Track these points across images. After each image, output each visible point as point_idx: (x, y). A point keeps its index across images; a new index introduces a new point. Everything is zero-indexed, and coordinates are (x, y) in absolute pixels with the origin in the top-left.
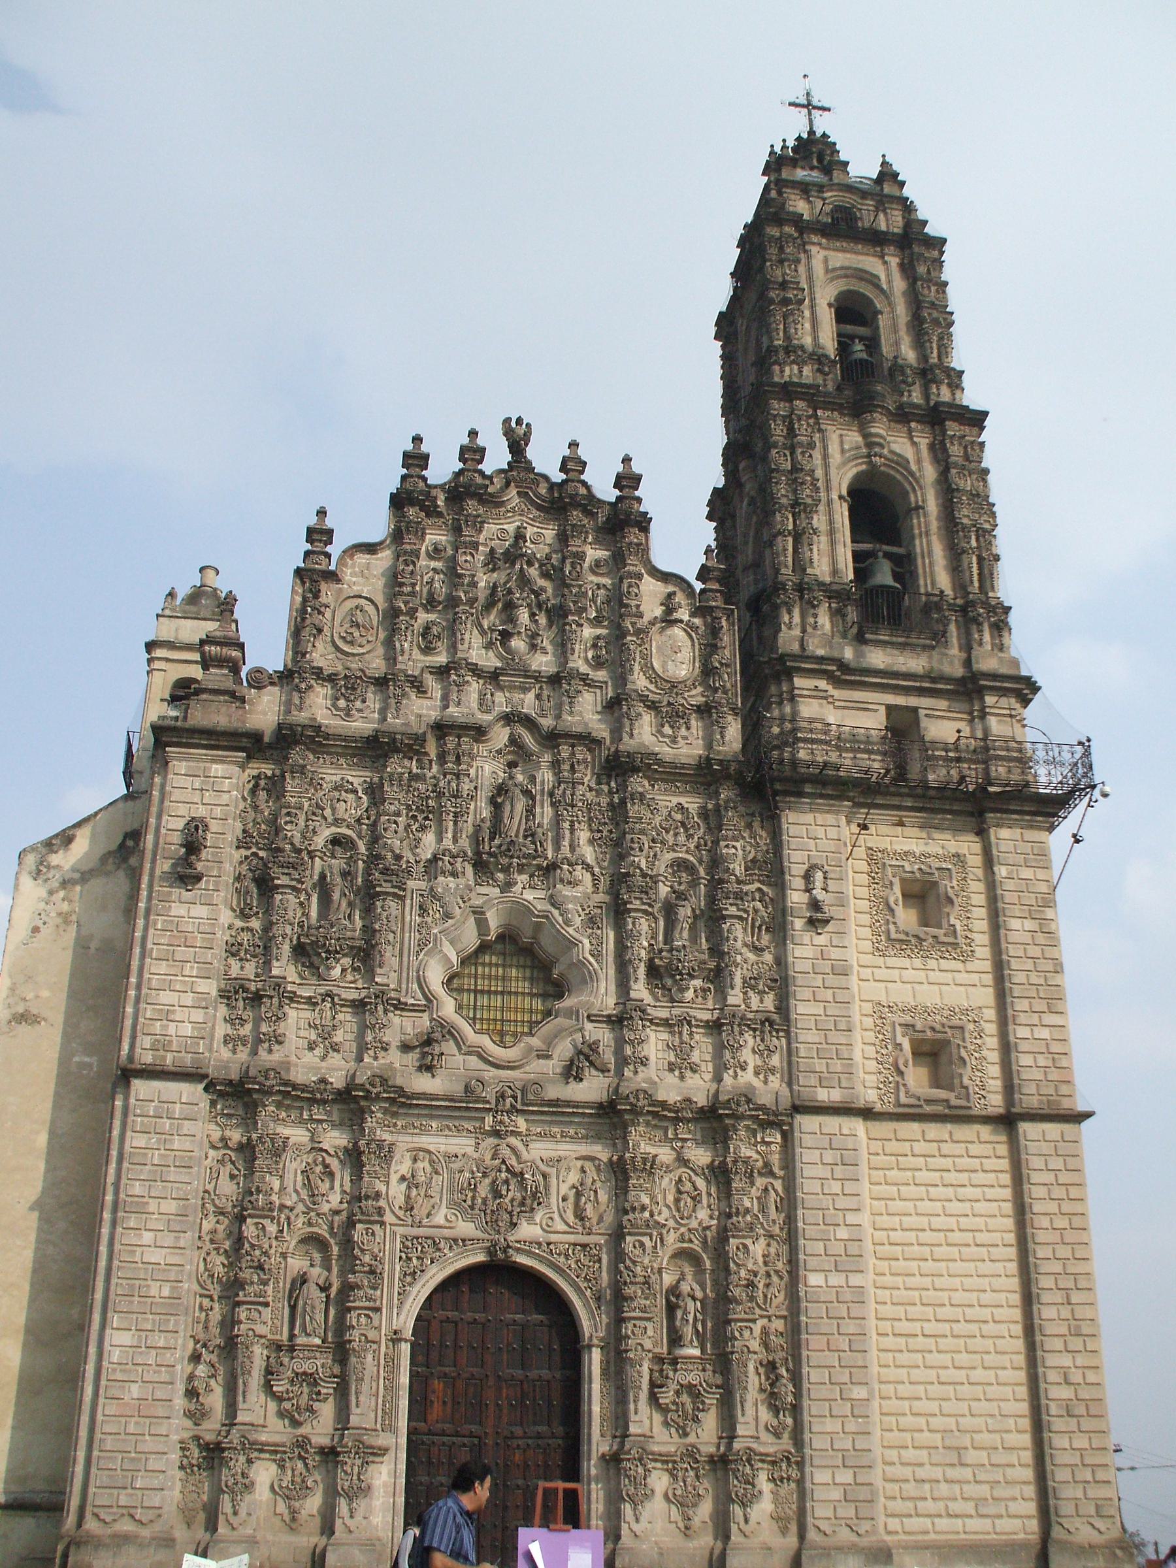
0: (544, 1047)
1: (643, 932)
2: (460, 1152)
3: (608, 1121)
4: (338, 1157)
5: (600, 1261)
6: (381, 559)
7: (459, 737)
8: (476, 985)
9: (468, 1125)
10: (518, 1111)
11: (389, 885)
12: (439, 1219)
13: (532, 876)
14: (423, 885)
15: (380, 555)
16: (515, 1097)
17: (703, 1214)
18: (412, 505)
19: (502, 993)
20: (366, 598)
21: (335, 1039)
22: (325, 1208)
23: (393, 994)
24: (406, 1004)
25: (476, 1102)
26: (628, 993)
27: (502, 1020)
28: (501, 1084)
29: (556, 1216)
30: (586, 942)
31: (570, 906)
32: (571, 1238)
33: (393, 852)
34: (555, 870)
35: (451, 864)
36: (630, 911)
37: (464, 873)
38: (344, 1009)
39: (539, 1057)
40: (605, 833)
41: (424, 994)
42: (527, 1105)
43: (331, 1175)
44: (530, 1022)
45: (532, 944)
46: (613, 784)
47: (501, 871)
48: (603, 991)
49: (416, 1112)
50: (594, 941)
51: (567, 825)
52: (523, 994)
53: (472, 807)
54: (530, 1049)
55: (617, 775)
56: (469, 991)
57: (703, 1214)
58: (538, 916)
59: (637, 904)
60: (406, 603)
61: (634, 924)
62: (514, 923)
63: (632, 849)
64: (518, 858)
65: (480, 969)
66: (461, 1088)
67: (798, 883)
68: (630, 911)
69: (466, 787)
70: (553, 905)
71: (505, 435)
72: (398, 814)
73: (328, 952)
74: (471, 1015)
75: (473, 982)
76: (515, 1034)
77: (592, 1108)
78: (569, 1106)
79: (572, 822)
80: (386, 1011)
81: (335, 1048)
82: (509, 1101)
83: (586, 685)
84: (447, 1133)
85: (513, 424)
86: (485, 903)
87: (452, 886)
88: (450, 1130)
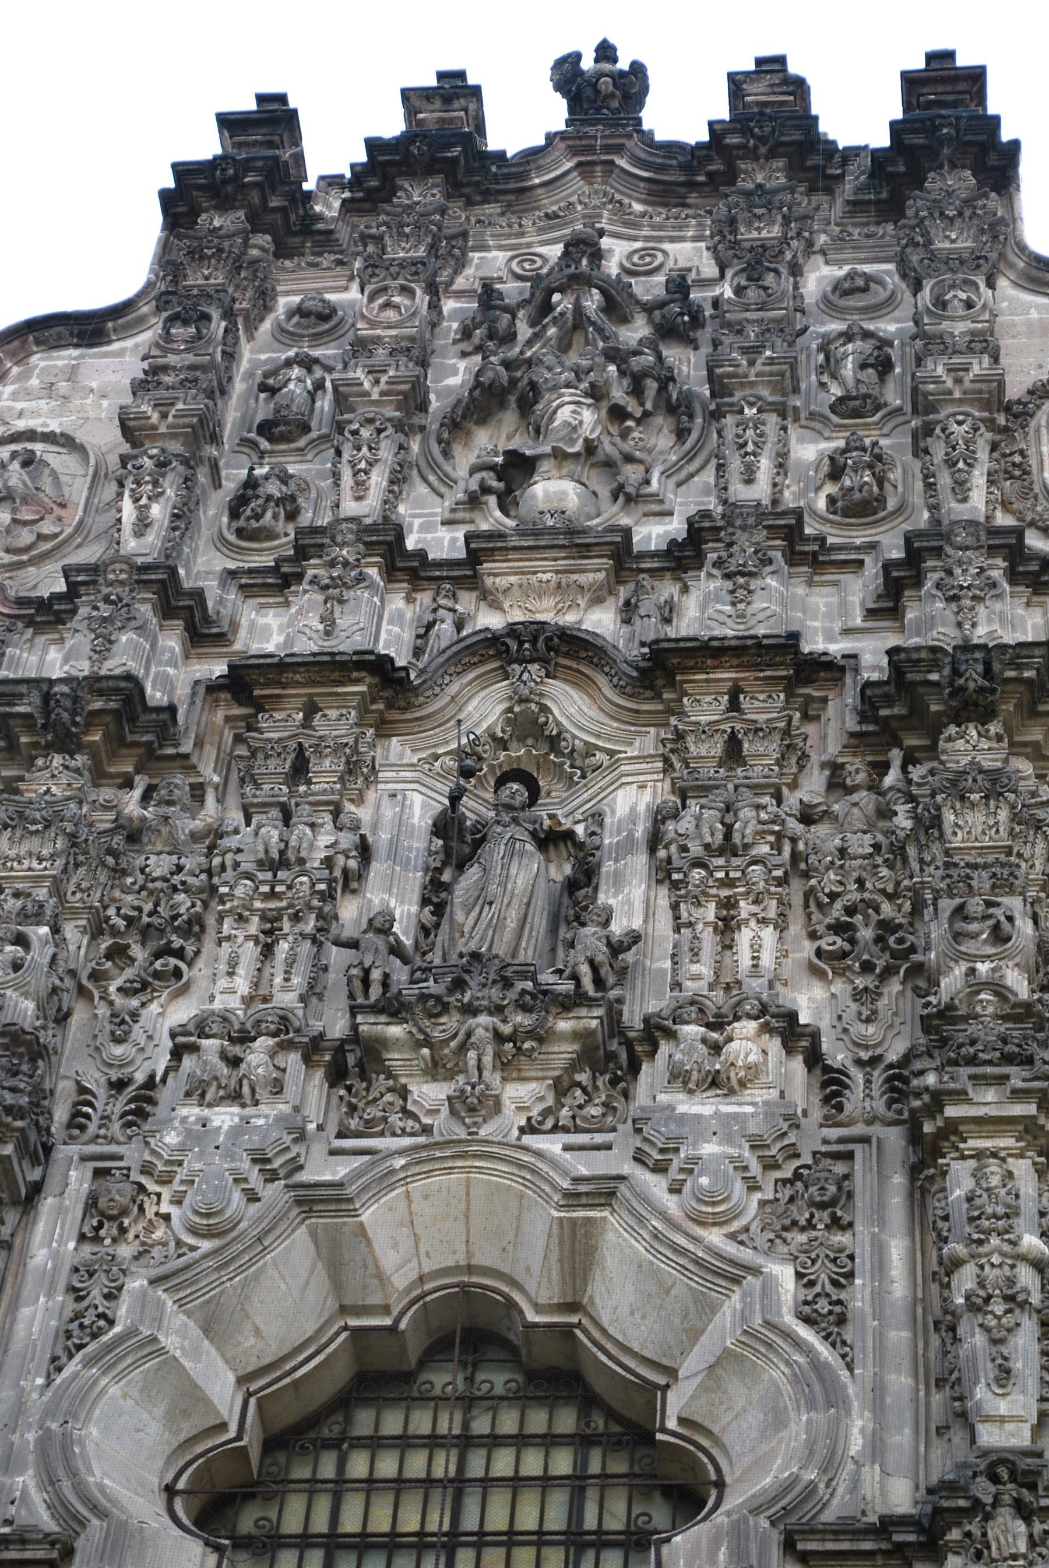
6: (121, 353)
7: (311, 709)
13: (561, 1089)
15: (116, 346)
18: (224, 205)
20: (49, 438)
30: (784, 1274)
31: (709, 1149)
34: (652, 1054)
35: (235, 1062)
36: (953, 1129)
37: (277, 1088)
40: (866, 934)
41: (59, 1507)
45: (566, 1332)
46: (891, 779)
47: (435, 1070)
48: (856, 1444)
55: (909, 760)
58: (572, 1198)
60: (163, 406)
64: (498, 1010)
68: (953, 1129)
69: (324, 839)
71: (558, 88)
79: (729, 904)
83: (794, 558)
85: (587, 63)
86: (357, 1174)
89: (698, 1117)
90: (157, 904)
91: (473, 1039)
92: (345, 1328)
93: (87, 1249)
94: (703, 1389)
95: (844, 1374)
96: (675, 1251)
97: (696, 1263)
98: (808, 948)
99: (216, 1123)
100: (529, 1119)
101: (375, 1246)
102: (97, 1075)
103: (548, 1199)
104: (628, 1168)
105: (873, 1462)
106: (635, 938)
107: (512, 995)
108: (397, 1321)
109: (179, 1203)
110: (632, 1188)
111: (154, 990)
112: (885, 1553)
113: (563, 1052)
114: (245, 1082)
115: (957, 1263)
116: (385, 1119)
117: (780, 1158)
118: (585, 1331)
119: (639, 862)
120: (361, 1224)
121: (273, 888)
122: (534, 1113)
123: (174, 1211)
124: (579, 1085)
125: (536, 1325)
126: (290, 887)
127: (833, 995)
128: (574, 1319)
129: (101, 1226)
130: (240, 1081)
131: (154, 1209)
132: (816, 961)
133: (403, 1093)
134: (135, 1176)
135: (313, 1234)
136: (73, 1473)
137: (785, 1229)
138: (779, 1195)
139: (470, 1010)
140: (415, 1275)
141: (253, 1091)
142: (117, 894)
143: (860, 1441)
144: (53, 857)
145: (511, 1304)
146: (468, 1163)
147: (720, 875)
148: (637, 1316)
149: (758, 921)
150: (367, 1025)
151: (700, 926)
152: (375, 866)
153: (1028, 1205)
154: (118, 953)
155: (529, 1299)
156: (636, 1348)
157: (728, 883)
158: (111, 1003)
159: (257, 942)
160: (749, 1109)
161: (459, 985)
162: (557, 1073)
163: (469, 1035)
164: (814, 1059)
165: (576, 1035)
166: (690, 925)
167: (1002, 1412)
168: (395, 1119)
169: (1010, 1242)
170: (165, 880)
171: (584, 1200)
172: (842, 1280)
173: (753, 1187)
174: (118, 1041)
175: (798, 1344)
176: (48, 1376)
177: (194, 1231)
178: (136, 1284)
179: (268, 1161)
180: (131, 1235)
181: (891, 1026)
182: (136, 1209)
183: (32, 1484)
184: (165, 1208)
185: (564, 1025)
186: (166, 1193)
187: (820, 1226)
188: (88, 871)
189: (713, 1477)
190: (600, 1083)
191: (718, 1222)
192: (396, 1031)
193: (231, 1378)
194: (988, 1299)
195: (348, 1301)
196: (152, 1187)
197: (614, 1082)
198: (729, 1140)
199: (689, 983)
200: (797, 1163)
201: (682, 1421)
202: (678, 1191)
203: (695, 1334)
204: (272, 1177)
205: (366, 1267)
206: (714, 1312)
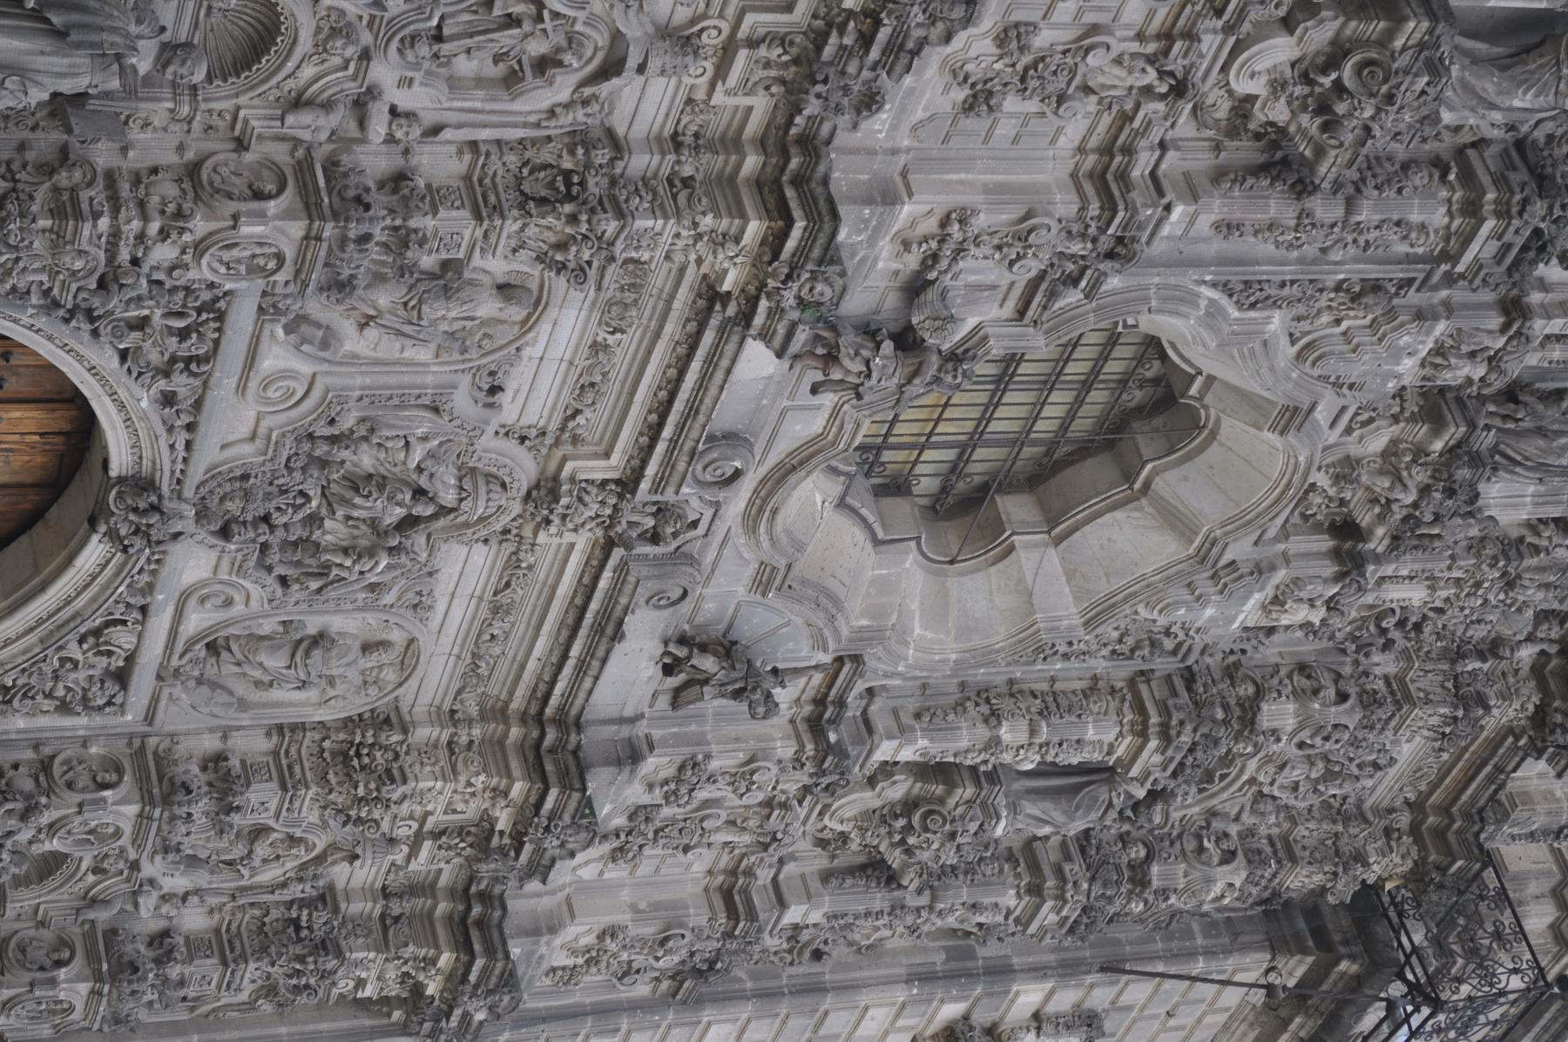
2: (505, 398)
3: (517, 704)
4: (567, 106)
5: (64, 708)
10: (609, 545)
12: (277, 356)
17: (178, 882)
21: (1011, 104)
22: (383, 72)
25: (668, 463)
29: (238, 608)
31: (1209, 612)
32: (153, 651)
36: (1143, 735)
38: (1107, 119)
43: (511, 80)
57: (178, 882)
59: (1151, 755)
62: (1214, 448)
66: (728, 411)
67: (1065, 1000)
73: (1339, 88)
78: (590, 651)
81: (980, 98)
96: (1130, 595)
97: (1113, 605)
112: (826, 695)
125: (1142, 467)
133: (1395, 419)
139: (1425, 491)
141: (1436, 366)
146: (1282, 486)
156: (1086, 529)
163: (1405, 486)
165: (1370, 532)
192: (1438, 446)
203: (1070, 575)
206: (1075, 597)
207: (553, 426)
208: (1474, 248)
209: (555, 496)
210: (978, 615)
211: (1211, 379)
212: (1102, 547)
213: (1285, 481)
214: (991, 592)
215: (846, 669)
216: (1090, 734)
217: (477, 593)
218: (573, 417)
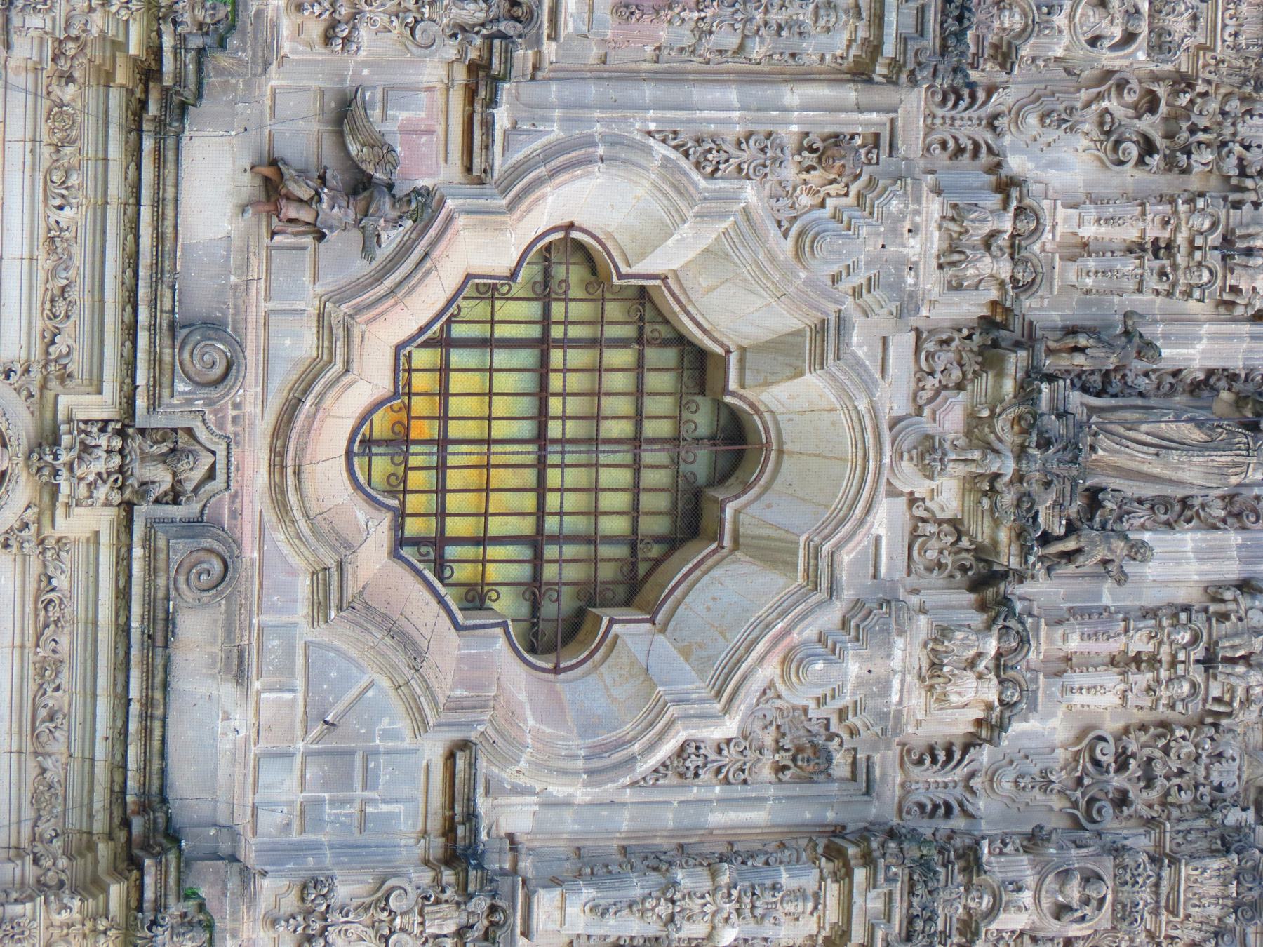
0: (351, 589)
1: (768, 930)
3: (100, 825)
8: (565, 343)
9: (74, 338)
11: (910, 29)
13: (955, 524)
14: (912, 143)
16: (175, 496)
19: (541, 438)
23: (525, 57)
24: (492, 102)
25: (155, 361)
26: (555, 882)
27: (443, 442)
28: (221, 454)
30: (729, 727)
31: (854, 668)
33: (1025, 34)
34: (982, 607)
35: (987, 243)
39: (320, 574)
40: (1117, 781)
42: (148, 542)
44: (440, 541)
45: (717, 537)
48: (558, 790)
49: (115, 151)
50: (730, 754)
51: (1140, 644)
52: (541, 513)
53: (1192, 306)
54: (346, 546)
56: (546, 321)
59: (869, 902)
61: (800, 894)
63: (1064, 875)
64: (1020, 477)
65: (621, 357)
70: (857, 604)
72: (1161, 44)
74: (458, 331)
75: (575, 332)
76: (398, 487)
77: (144, 770)
79: (1154, 661)
80: (460, 30)
82: (162, 477)
84: (44, 263)
87: (913, 247)
88: (52, 274)
89: (889, 656)
90: (1206, 130)
91: (990, 456)
92: (728, 352)
93: (791, 144)
94: (633, 662)
95: (628, 780)
98: (1110, 726)
99: (912, 242)
100: (923, 500)
101: (788, 384)
102: (1011, 101)
103: (818, 531)
104: (848, 594)
105: (542, 805)
106: (1122, 578)
107: (1035, 488)
108: (733, 394)
109: (834, 217)
110: (820, 604)
111: (1102, 142)
112: (452, 818)
113: (982, 530)
114: (963, 257)
115: (714, 875)
116: (931, 374)
117: (847, 722)
118: (714, 552)
119: (1232, 570)
120: (802, 374)
121: (1199, 248)
122: (929, 504)
123: (827, 212)
124: (959, 539)
125: (723, 511)
126: (1200, 264)
127: (1053, 750)
128: (727, 542)
129: (812, 150)
130: (963, 253)
131: (833, 193)
132: (1091, 735)
133: (960, 387)
134: (868, 171)
135: (798, 333)
136: (553, 174)
137: (778, 727)
138: (814, 721)
139: (1021, 453)
140: (774, 409)
141: (953, 264)
142: (1223, 91)
143: (561, 795)
144: (1236, 47)
145: (747, 487)
146: (860, 462)
147: (1182, 656)
148: (710, 603)
149: (1125, 691)
150: (1016, 362)
151: (1123, 639)
152: (1246, 328)
153: (768, 930)
154: (1152, 103)
155: (747, 505)
156: (688, 600)
157: (1173, 663)
158: (1088, 104)
159: (1143, 236)
160: (895, 698)
161: (1044, 444)
162: (966, 522)
164: (971, 743)
165: (995, 543)
166: (1126, 631)
167: (569, 910)
168: (931, 382)
169: (727, 920)
170: (1234, 134)
171: (812, 562)
172: (721, 776)
173: (820, 701)
174: (1042, 118)
175: (652, 747)
176: (659, 132)
177: (802, 234)
178: (750, 193)
179: (869, 291)
180: (805, 176)
181: (1014, 801)
182: (832, 176)
183: (551, 138)
184: (830, 202)
185: (1003, 536)
186: (851, 199)
187: (777, 757)
188: (1240, 68)
189: (562, 666)
190: (964, 555)
191: (785, 675)
192: (1009, 386)
193: (675, 267)
194: (673, 902)
195: (748, 354)
196: (854, 189)
197: (964, 569)
198: (861, 683)
199: (1060, 632)
200: (845, 736)
201: (616, 637)
202: (820, 641)
203: (686, 653)
204: (856, 293)
205: (773, 374)
207: (37, 354)
208: (891, 18)
209: (56, 442)
210: (599, 712)
211: (743, 350)
212: (709, 609)
213: (860, 454)
214: (607, 689)
215: (460, 763)
216: (785, 878)
217: (17, 643)
218: (53, 342)
